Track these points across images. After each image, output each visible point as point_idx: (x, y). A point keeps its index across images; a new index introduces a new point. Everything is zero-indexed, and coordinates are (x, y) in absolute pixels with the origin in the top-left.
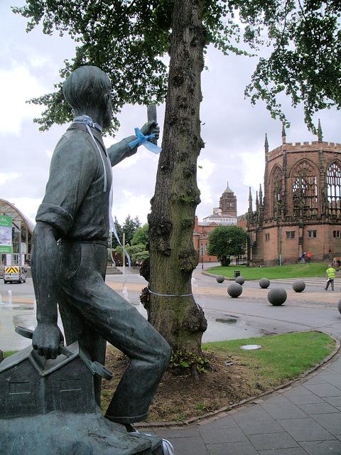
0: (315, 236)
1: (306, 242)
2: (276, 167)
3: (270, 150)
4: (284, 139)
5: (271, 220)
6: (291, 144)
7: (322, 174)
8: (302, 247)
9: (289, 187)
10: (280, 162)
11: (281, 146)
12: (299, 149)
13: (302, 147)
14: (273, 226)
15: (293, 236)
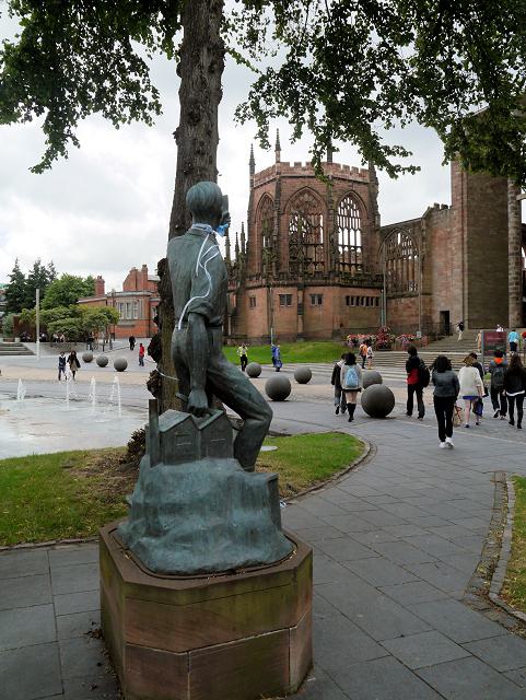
0: (320, 302)
1: (308, 311)
2: (265, 198)
3: (258, 170)
4: (278, 156)
5: (258, 276)
6: (288, 164)
7: (331, 212)
8: (303, 319)
9: (283, 228)
10: (271, 189)
11: (274, 166)
12: (300, 172)
13: (304, 169)
14: (260, 287)
15: (289, 303)
